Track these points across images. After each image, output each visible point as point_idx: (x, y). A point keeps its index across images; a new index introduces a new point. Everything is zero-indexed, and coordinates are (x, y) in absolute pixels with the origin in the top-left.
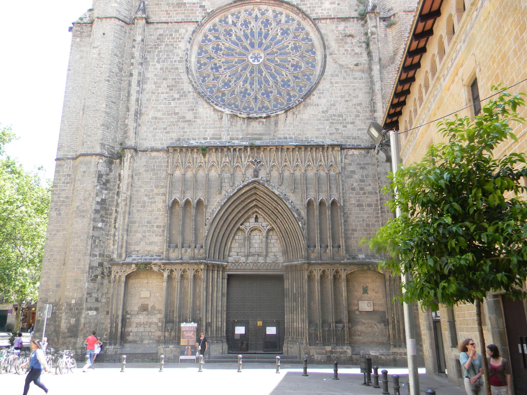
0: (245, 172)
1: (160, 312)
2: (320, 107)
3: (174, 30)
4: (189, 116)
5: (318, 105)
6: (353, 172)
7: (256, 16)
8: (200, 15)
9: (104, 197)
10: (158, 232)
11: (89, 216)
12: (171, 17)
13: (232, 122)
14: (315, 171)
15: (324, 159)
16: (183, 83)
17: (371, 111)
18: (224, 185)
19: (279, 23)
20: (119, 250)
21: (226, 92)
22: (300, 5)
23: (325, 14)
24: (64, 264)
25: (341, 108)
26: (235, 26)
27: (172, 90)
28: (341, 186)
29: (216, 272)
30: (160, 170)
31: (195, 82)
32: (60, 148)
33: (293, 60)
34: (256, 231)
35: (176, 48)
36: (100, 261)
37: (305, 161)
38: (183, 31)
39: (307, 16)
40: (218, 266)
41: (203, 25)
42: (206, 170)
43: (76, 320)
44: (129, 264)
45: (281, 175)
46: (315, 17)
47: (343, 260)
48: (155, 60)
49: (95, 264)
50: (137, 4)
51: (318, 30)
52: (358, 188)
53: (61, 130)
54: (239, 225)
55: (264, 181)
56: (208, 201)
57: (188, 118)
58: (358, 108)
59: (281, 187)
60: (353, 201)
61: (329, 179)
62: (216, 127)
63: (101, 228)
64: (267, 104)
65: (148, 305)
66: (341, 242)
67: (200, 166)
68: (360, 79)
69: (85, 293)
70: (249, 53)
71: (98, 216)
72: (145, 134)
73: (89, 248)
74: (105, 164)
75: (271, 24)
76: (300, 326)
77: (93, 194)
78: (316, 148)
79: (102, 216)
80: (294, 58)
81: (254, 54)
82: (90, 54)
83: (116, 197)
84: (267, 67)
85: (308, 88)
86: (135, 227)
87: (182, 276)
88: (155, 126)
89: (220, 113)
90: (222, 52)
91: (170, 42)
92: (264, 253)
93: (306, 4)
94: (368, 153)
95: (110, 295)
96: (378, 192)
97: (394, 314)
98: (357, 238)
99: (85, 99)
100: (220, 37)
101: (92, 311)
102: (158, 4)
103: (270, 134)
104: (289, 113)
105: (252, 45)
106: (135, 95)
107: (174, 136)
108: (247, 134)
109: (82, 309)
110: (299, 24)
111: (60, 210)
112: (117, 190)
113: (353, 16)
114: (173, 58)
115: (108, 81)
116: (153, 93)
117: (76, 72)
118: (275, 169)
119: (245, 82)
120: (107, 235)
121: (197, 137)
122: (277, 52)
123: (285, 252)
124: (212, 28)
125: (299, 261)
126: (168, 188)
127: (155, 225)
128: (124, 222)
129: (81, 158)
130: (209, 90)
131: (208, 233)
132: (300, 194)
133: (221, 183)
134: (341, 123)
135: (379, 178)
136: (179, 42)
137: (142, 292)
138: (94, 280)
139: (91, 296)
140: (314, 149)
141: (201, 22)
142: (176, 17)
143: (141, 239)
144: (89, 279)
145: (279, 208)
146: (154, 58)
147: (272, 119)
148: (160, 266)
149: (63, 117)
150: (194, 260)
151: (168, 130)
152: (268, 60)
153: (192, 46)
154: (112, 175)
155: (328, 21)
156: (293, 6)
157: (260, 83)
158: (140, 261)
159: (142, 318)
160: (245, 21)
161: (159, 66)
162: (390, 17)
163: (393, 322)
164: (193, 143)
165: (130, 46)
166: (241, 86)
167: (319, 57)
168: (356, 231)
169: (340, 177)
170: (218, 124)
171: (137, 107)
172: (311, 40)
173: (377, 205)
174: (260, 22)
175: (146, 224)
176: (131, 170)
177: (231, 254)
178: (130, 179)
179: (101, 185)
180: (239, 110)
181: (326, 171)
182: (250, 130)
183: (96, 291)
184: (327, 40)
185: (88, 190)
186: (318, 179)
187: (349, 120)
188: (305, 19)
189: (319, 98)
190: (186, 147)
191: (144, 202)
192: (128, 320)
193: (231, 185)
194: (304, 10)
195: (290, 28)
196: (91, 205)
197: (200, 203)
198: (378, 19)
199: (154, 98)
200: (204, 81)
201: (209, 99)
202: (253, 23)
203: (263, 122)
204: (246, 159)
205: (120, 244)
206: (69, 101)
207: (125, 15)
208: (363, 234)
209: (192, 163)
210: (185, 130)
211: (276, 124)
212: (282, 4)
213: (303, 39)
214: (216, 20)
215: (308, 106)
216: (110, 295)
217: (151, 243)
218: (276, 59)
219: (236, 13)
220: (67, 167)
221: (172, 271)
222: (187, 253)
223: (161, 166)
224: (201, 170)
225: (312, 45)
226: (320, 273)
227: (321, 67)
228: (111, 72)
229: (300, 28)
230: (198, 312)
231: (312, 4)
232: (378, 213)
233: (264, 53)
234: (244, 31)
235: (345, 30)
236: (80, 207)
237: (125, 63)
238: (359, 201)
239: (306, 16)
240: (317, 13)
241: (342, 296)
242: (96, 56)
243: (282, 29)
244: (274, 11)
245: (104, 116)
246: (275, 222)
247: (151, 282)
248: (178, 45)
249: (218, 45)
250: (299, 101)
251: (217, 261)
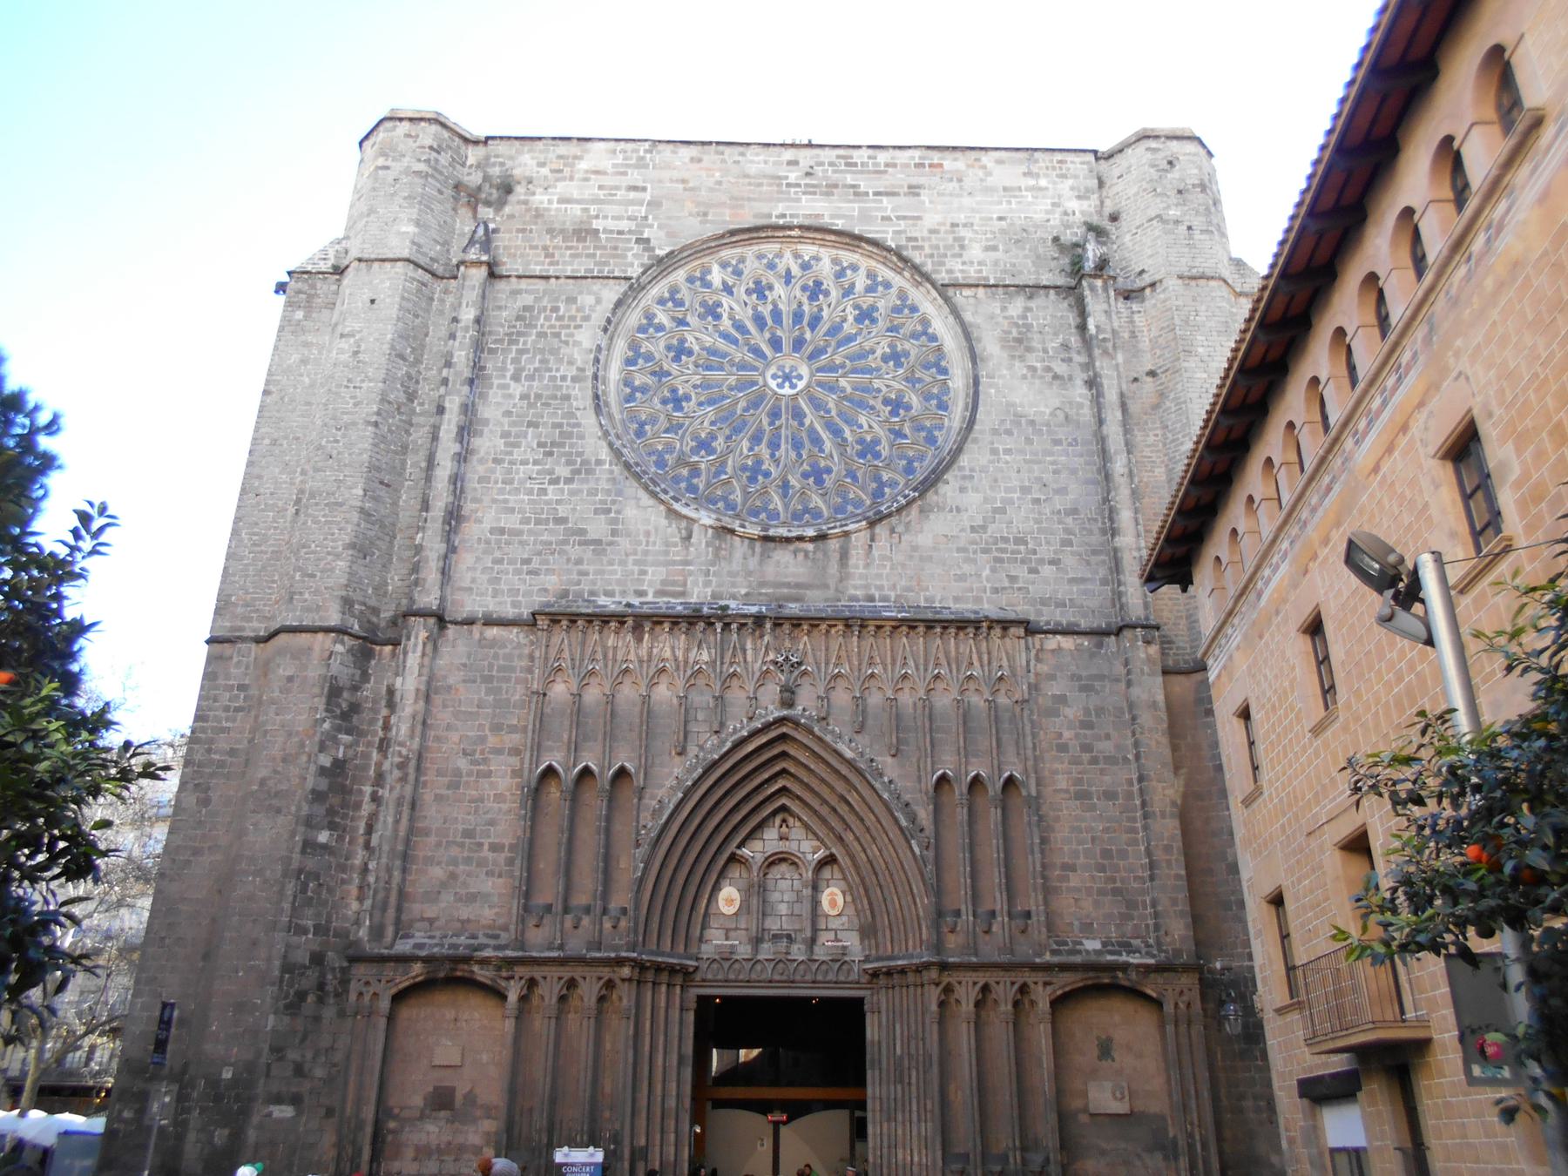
0: (755, 692)
1: (489, 1112)
2: (965, 516)
3: (564, 297)
4: (598, 528)
5: (958, 510)
6: (1062, 699)
7: (788, 272)
8: (636, 263)
9: (340, 755)
10: (495, 863)
11: (293, 809)
12: (557, 263)
13: (718, 549)
14: (954, 694)
15: (980, 659)
16: (582, 437)
17: (1103, 532)
18: (693, 727)
19: (848, 291)
20: (377, 914)
21: (703, 466)
22: (906, 248)
23: (972, 273)
24: (206, 957)
25: (1021, 519)
26: (731, 293)
27: (551, 454)
28: (1029, 739)
29: (664, 988)
30: (508, 680)
31: (618, 437)
32: (223, 606)
33: (887, 386)
34: (784, 867)
35: (566, 343)
36: (316, 947)
37: (926, 665)
38: (589, 300)
39: (927, 277)
40: (672, 970)
41: (644, 288)
42: (643, 684)
43: (230, 1135)
44: (405, 960)
45: (859, 701)
46: (946, 282)
47: (1040, 955)
48: (509, 374)
49: (302, 957)
50: (467, 229)
51: (955, 312)
52: (1074, 748)
53: (229, 557)
54: (732, 847)
55: (810, 717)
56: (646, 774)
57: (592, 536)
58: (1069, 520)
59: (858, 738)
60: (1062, 783)
61: (996, 717)
62: (674, 563)
63: (324, 847)
64: (816, 501)
65: (452, 1090)
66: (1032, 901)
67: (627, 670)
68: (1070, 444)
69: (266, 1048)
70: (767, 366)
71: (320, 810)
72: (469, 575)
73: (286, 906)
74: (351, 658)
75: (827, 293)
76: (916, 1159)
77: (311, 745)
78: (959, 628)
79: (331, 812)
80: (890, 382)
81: (781, 368)
82: (330, 351)
83: (375, 755)
84: (817, 405)
85: (929, 462)
86: (425, 847)
87: (562, 999)
88: (498, 554)
89: (684, 524)
90: (693, 359)
91: (552, 327)
92: (809, 934)
93: (921, 248)
94: (1100, 645)
95: (338, 1057)
96: (1130, 756)
97: (1192, 1124)
98: (1078, 890)
99: (303, 473)
100: (689, 319)
101: (283, 1107)
102: (523, 231)
103: (826, 586)
104: (878, 529)
105: (776, 344)
106: (449, 464)
107: (552, 582)
108: (762, 584)
109: (252, 1099)
110: (902, 295)
111: (209, 788)
112: (381, 733)
113: (1045, 283)
114: (558, 370)
115: (376, 424)
116: (496, 461)
117: (286, 400)
118: (841, 684)
119: (756, 439)
120: (343, 868)
121: (617, 589)
122: (843, 366)
123: (867, 932)
124: (667, 295)
125: (912, 956)
126: (530, 734)
127: (486, 842)
128: (396, 830)
129: (283, 638)
130: (654, 458)
131: (645, 868)
132: (914, 760)
133: (686, 723)
134: (1023, 561)
135: (1134, 719)
136: (577, 327)
138: (293, 1006)
139: (281, 1059)
140: (953, 630)
141: (638, 279)
142: (572, 264)
143: (444, 884)
144: (281, 1004)
145: (853, 798)
146: (504, 369)
147: (834, 545)
148: (499, 969)
149: (237, 520)
150: (599, 950)
151: (534, 565)
152: (820, 384)
153: (611, 339)
154: (367, 691)
155: (981, 291)
156: (889, 250)
157: (797, 445)
158: (436, 950)
159: (433, 1131)
160: (757, 283)
161: (517, 389)
162: (1143, 289)
163: (1191, 1147)
164: (608, 603)
165: (443, 332)
166: (745, 451)
167: (958, 381)
168: (1073, 868)
169: (1026, 713)
170: (677, 553)
171: (451, 499)
172: (933, 338)
173: (1129, 796)
174: (798, 287)
175: (459, 839)
176: (424, 678)
177: (709, 933)
178: (421, 703)
179: (335, 717)
180: (737, 516)
181: (987, 695)
182: (770, 571)
183: (297, 1041)
184: (979, 340)
185: (297, 732)
186: (965, 716)
187: (1045, 552)
188: (920, 284)
189: (962, 490)
190: (588, 615)
191: (457, 773)
192: (390, 1138)
193: (716, 728)
194: (917, 261)
195: (879, 305)
196: (304, 776)
197: (622, 773)
198: (1112, 293)
199: (499, 474)
200: (640, 433)
201: (656, 484)
202: (779, 289)
203: (806, 553)
204: (756, 653)
205: (381, 895)
206: (260, 477)
207: (432, 254)
208: (1093, 877)
209: (601, 663)
210: (584, 567)
211: (844, 555)
212: (856, 243)
213: (915, 336)
214: (679, 276)
215: (931, 511)
216: (338, 1057)
217: (472, 898)
218: (843, 382)
219: (734, 262)
220: (239, 662)
221: (532, 983)
222: (580, 930)
223: (513, 669)
224: (628, 681)
225: (939, 349)
226: (974, 993)
227: (966, 409)
228: (384, 400)
229: (904, 306)
230: (607, 1114)
231: (937, 247)
232: (1134, 820)
233: (810, 366)
234: (755, 308)
235: (1025, 317)
236: (271, 783)
237: (425, 379)
238: (1079, 781)
239: (921, 275)
240: (950, 272)
241: (1041, 1066)
242: (345, 357)
243: (856, 307)
244: (835, 261)
245: (355, 520)
246: (841, 839)
247: (466, 1016)
248: (572, 335)
249: (682, 341)
250: (905, 497)
251: (669, 956)
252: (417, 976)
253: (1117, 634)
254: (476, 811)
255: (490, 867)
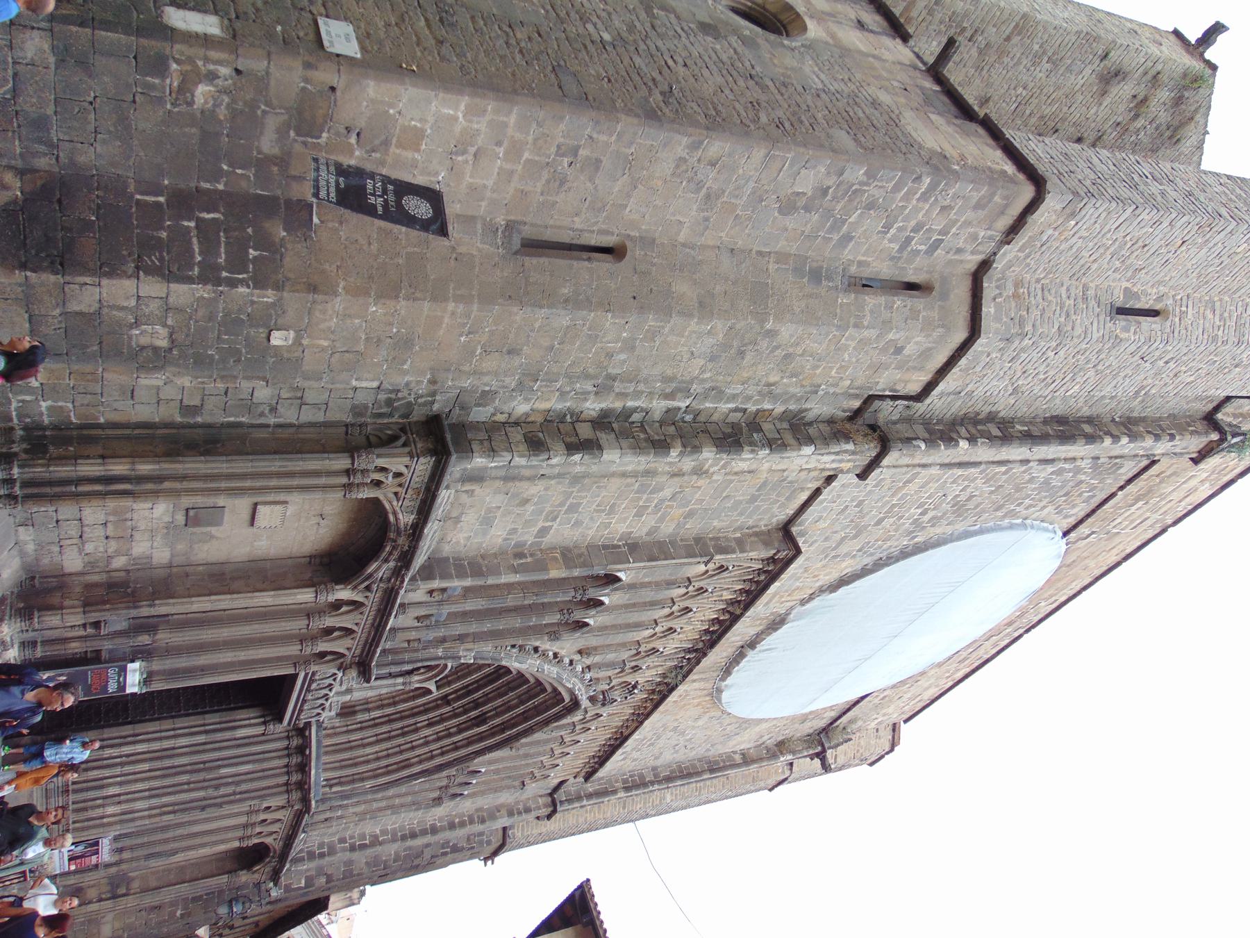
43: (156, 349)
129: (961, 335)
137: (278, 508)
185: (816, 367)
205: (527, 473)
236: (764, 344)
252: (397, 519)
253: (551, 795)
254: (597, 511)
255: (520, 531)
